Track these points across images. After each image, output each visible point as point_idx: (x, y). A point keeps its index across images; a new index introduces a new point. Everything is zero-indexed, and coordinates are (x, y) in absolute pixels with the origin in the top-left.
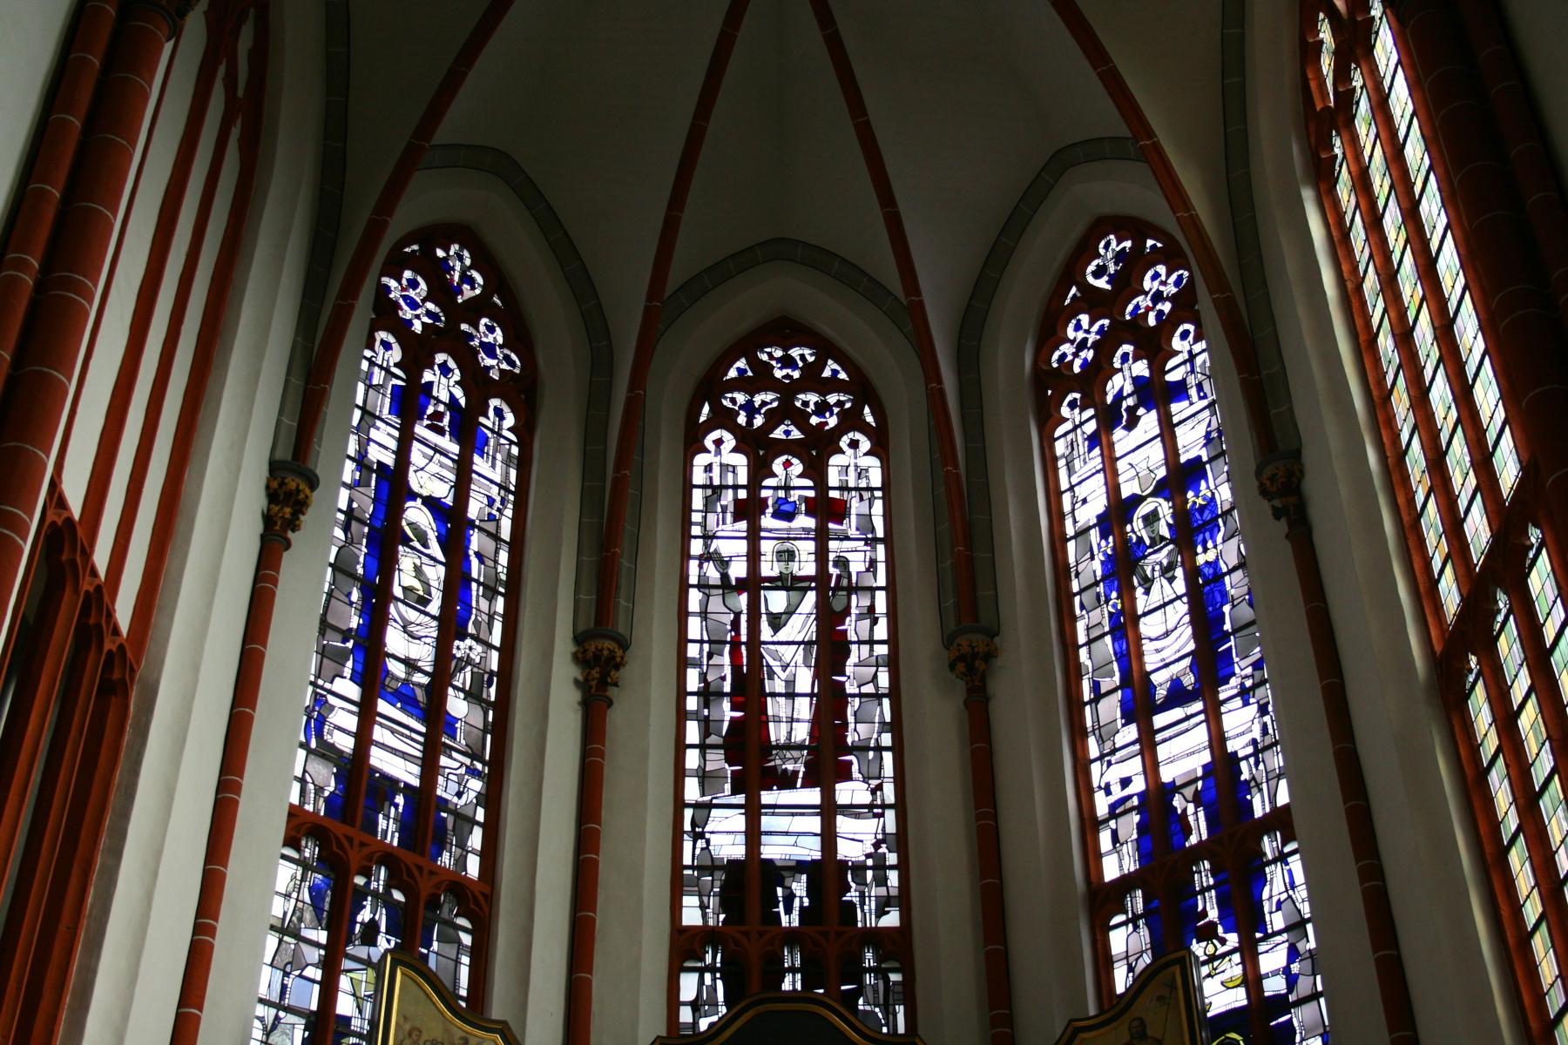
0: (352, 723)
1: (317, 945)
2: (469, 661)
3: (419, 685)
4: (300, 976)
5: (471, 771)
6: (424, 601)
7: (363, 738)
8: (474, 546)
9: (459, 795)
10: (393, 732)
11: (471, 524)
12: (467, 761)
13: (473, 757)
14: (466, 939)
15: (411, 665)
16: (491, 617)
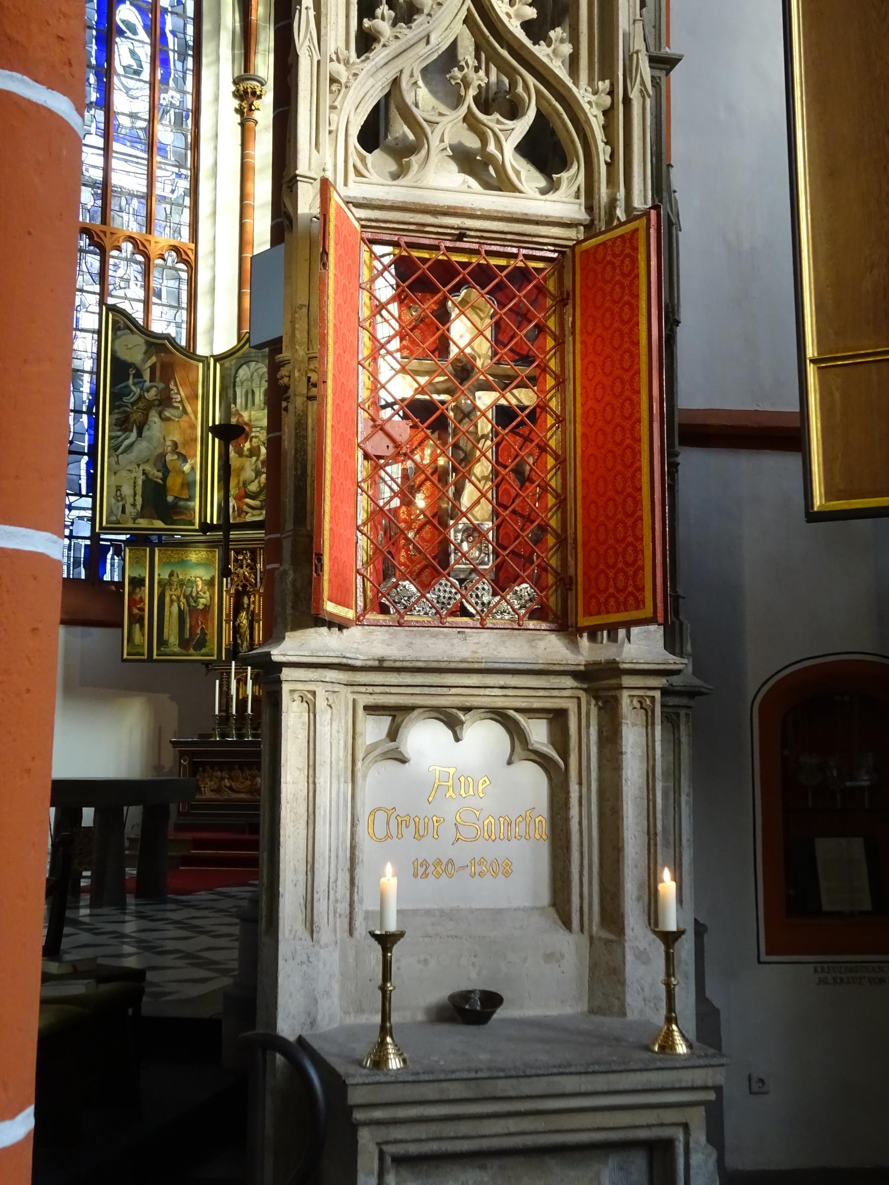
0: (100, 161)
1: (95, 293)
2: (172, 105)
3: (140, 129)
4: (87, 311)
5: (179, 175)
6: (137, 73)
7: (107, 170)
8: (169, 27)
9: (173, 191)
10: (126, 161)
11: (165, 11)
12: (176, 170)
13: (179, 166)
14: (184, 275)
15: (133, 116)
16: (184, 73)
